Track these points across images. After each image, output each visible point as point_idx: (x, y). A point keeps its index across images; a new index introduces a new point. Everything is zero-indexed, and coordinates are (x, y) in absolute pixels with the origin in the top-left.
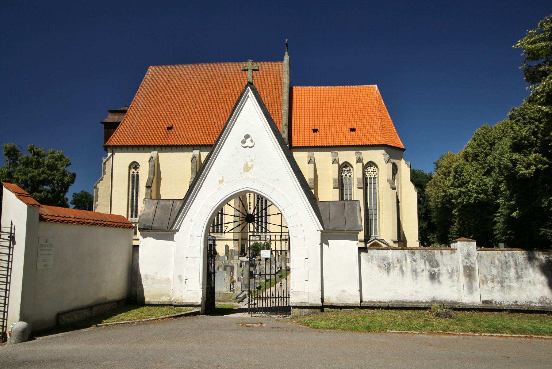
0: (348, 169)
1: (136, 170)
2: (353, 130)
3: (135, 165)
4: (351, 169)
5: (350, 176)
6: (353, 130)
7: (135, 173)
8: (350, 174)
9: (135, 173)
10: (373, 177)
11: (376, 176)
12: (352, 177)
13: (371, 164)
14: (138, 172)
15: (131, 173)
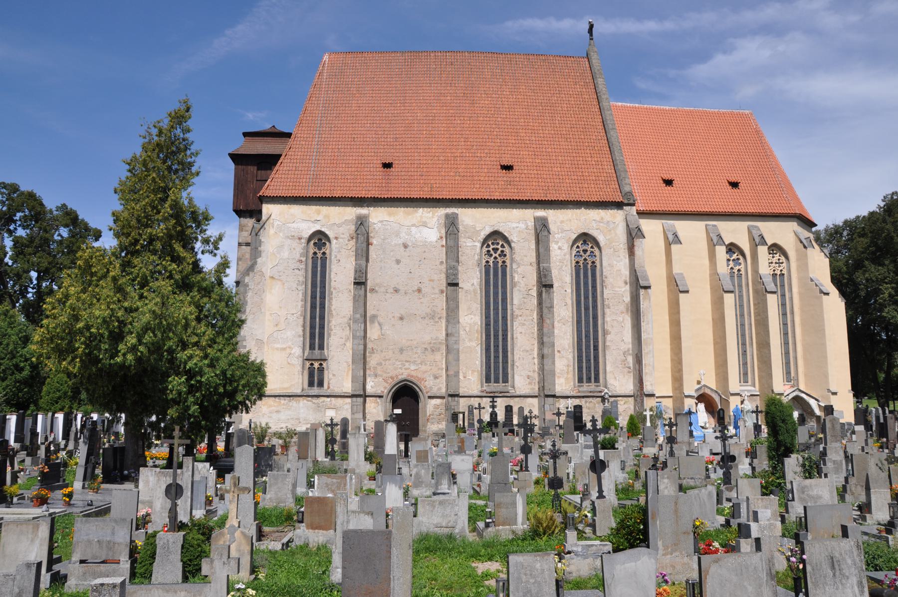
0: (735, 256)
1: (320, 249)
2: (734, 185)
3: (320, 239)
4: (740, 257)
5: (739, 270)
6: (734, 185)
7: (319, 255)
8: (738, 268)
9: (319, 255)
10: (778, 273)
11: (785, 272)
12: (743, 272)
13: (775, 248)
14: (324, 253)
15: (311, 255)
